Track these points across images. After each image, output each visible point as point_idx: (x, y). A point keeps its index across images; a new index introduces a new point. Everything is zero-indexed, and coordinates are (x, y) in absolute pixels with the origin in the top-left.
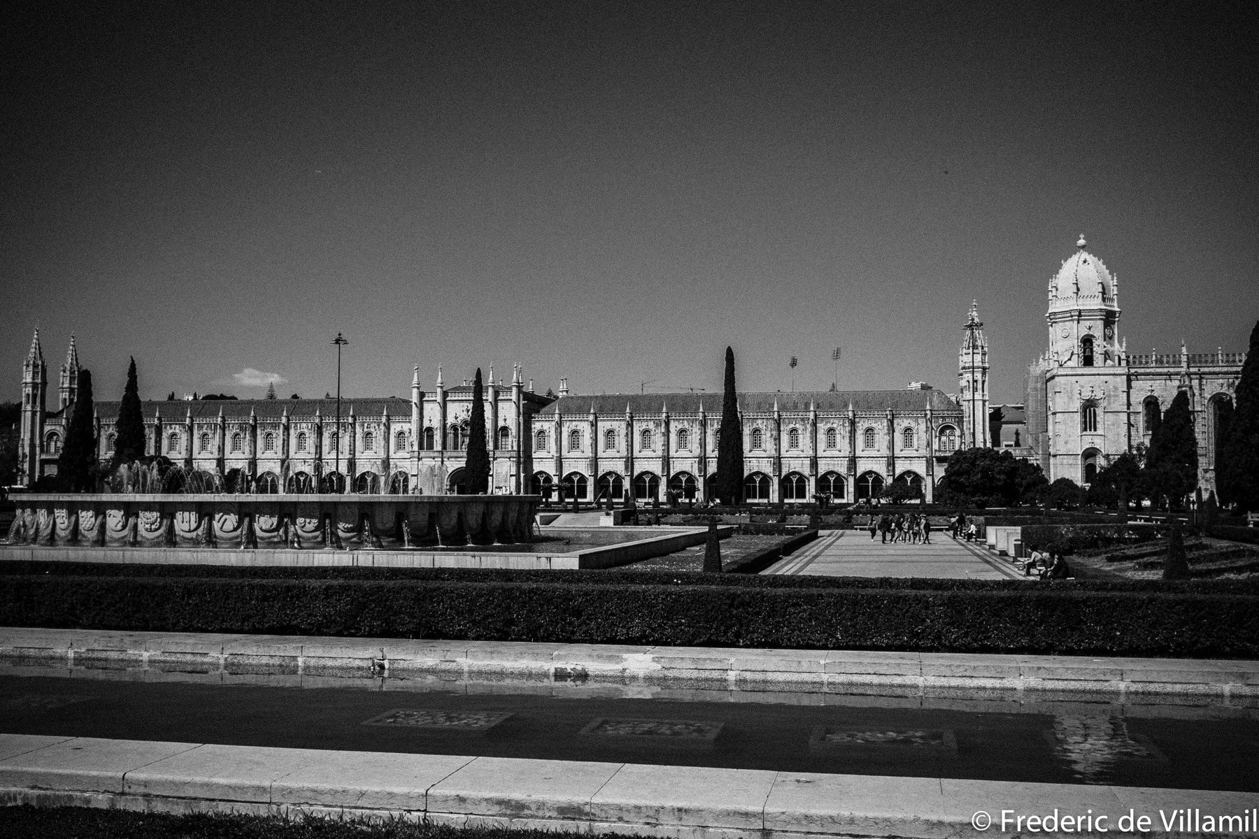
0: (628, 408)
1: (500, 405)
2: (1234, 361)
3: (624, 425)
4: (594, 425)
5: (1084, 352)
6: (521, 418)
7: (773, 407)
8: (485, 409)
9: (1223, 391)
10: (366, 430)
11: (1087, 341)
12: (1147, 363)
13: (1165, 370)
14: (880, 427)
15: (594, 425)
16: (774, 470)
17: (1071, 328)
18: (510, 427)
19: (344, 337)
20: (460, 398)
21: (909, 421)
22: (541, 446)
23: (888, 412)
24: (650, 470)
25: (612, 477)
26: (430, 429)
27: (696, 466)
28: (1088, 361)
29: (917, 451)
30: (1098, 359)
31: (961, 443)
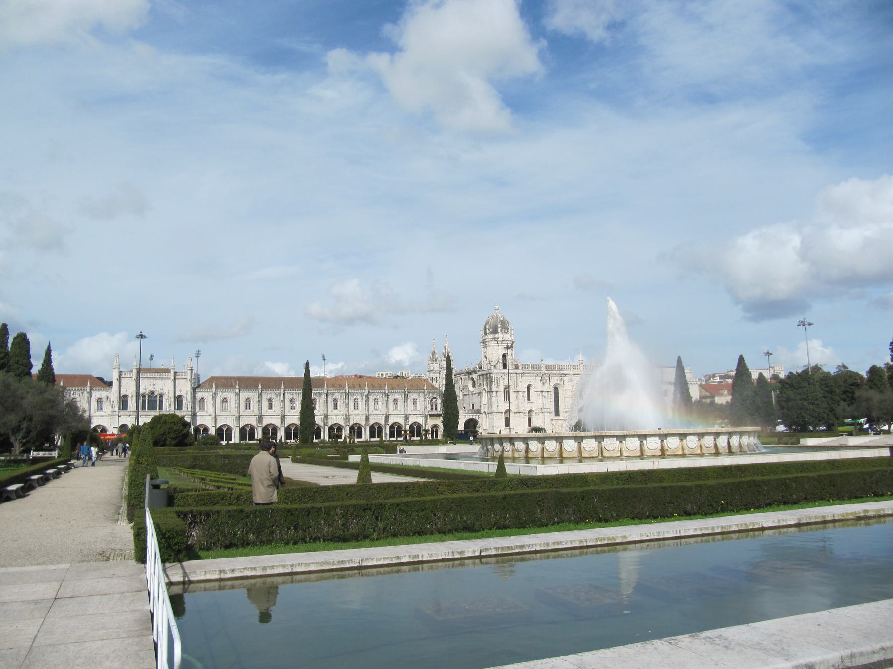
0: (260, 385)
1: (177, 380)
2: (562, 368)
3: (257, 395)
4: (238, 395)
5: (503, 362)
6: (192, 390)
9: (558, 382)
11: (504, 356)
12: (528, 368)
13: (536, 372)
14: (401, 398)
15: (238, 395)
16: (346, 422)
17: (498, 350)
18: (184, 395)
19: (144, 334)
20: (148, 376)
22: (202, 408)
23: (406, 390)
24: (272, 423)
25: (248, 427)
26: (125, 396)
28: (504, 366)
30: (510, 366)
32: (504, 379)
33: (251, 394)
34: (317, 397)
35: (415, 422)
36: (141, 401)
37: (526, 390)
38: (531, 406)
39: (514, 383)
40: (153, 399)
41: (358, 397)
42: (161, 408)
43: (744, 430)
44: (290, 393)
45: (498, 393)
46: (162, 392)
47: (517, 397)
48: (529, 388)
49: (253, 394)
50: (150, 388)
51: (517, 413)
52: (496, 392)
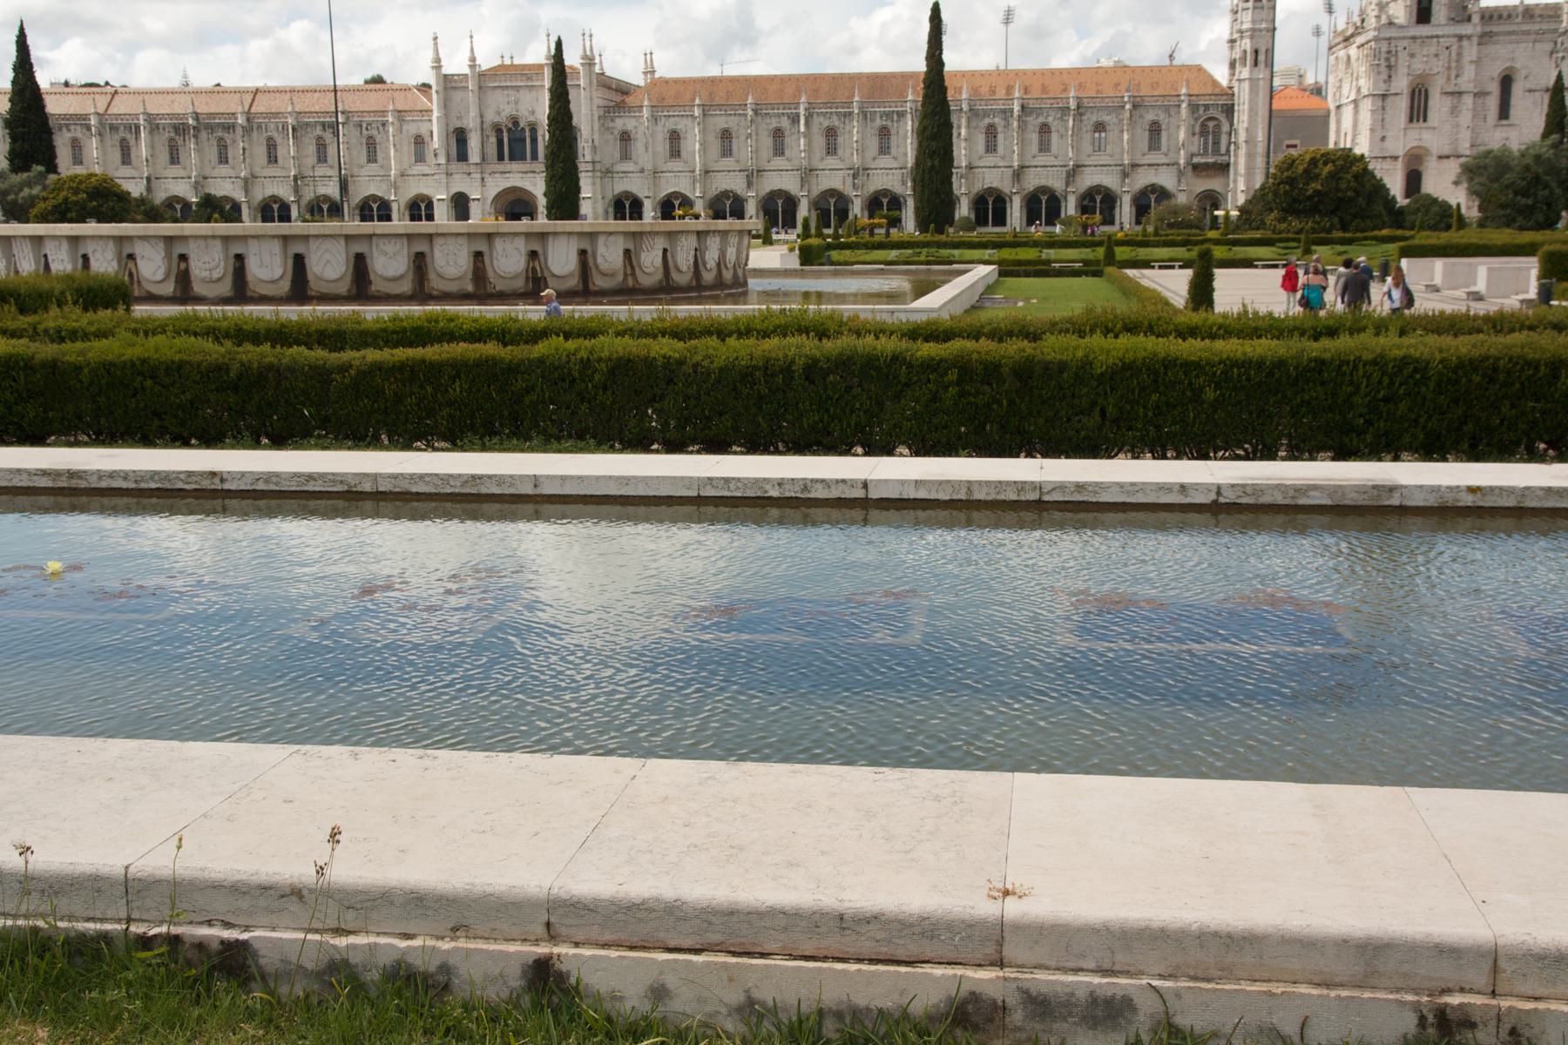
7: (960, 93)
8: (571, 97)
10: (365, 132)
12: (1509, 16)
13: (1536, 27)
21: (1156, 111)
25: (728, 198)
27: (849, 181)
29: (1166, 155)
31: (1230, 143)
32: (1412, 56)
33: (732, 118)
34: (889, 123)
35: (1153, 185)
36: (493, 140)
37: (1494, 88)
38: (1504, 135)
39: (1449, 68)
40: (518, 136)
41: (997, 120)
42: (535, 157)
43: (232, 233)
44: (824, 114)
45: (1390, 100)
46: (532, 119)
47: (1454, 111)
48: (1506, 82)
49: (736, 118)
50: (508, 110)
51: (1448, 157)
52: (1384, 97)
